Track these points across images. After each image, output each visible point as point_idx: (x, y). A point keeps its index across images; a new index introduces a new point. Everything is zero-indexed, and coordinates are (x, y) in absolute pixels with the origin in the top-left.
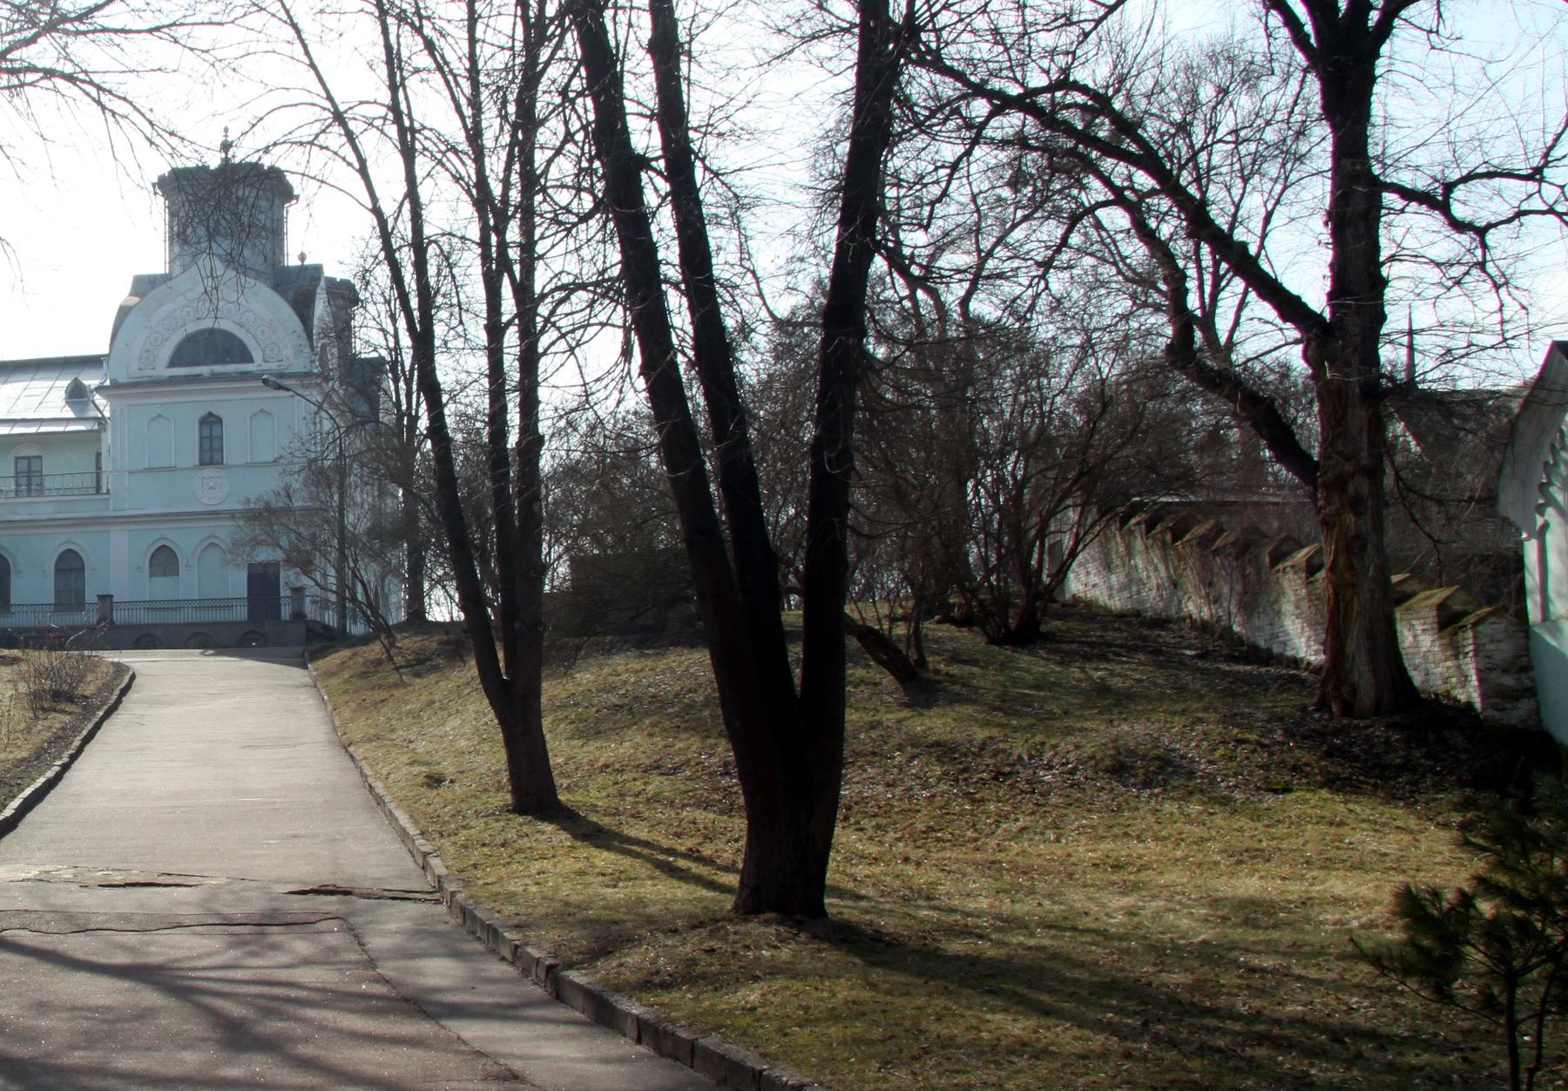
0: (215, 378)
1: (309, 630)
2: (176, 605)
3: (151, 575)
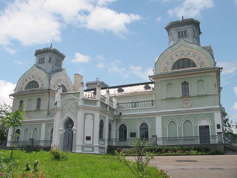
1: (225, 147)
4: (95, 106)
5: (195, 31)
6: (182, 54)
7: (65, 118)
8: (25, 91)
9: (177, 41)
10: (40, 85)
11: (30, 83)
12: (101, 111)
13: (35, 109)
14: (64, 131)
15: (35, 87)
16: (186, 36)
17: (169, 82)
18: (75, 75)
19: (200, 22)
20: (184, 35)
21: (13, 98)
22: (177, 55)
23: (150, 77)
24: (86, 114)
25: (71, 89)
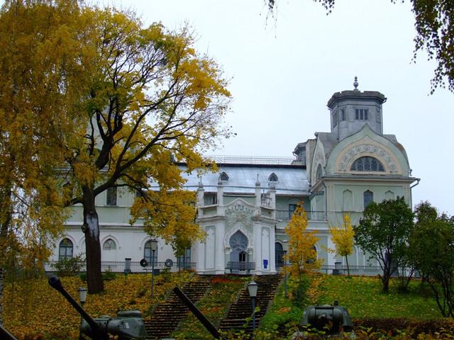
4: (268, 217)
6: (367, 149)
13: (106, 204)
14: (231, 250)
16: (366, 119)
20: (364, 117)
24: (263, 228)
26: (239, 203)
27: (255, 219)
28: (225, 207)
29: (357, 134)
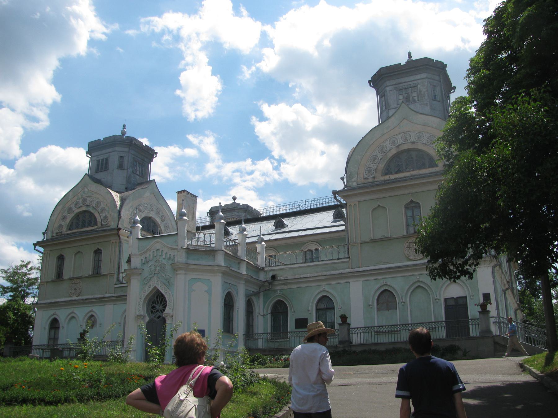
0: (412, 178)
1: (496, 343)
2: (393, 330)
3: (379, 310)
5: (436, 86)
6: (406, 139)
7: (148, 290)
8: (68, 234)
9: (395, 110)
10: (99, 220)
11: (77, 216)
12: (224, 273)
14: (147, 319)
15: (89, 225)
17: (378, 203)
18: (178, 193)
19: (446, 65)
20: (411, 98)
21: (42, 249)
22: (393, 142)
23: (335, 193)
25: (170, 226)
26: (158, 246)
27: (175, 268)
28: (141, 255)
29: (389, 120)
